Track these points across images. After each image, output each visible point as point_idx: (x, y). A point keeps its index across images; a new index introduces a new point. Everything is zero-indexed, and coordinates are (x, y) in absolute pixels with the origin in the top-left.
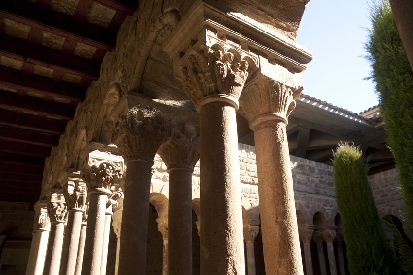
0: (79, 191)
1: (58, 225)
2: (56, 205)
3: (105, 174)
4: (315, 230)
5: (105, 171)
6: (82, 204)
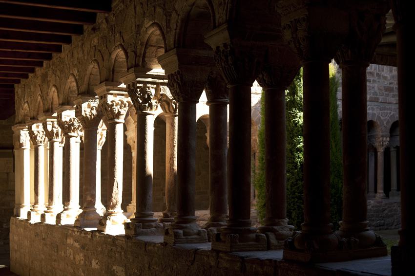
0: (55, 128)
1: (39, 148)
2: (36, 133)
3: (73, 125)
5: (73, 123)
6: (58, 136)
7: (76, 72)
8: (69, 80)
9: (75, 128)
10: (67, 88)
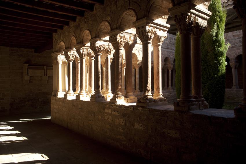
0: (84, 52)
2: (69, 55)
3: (100, 49)
4: (165, 64)
7: (110, 18)
8: (101, 24)
9: (101, 50)
10: (99, 29)
